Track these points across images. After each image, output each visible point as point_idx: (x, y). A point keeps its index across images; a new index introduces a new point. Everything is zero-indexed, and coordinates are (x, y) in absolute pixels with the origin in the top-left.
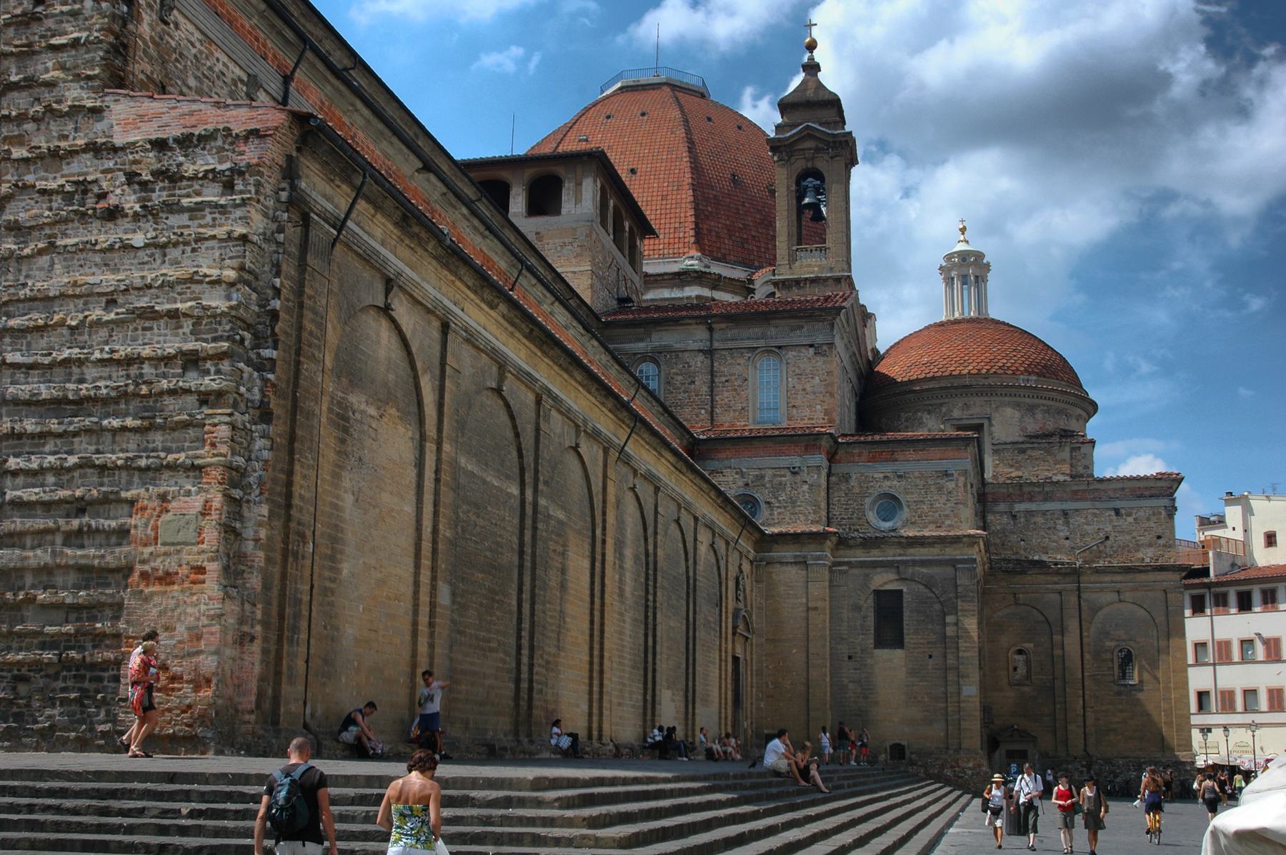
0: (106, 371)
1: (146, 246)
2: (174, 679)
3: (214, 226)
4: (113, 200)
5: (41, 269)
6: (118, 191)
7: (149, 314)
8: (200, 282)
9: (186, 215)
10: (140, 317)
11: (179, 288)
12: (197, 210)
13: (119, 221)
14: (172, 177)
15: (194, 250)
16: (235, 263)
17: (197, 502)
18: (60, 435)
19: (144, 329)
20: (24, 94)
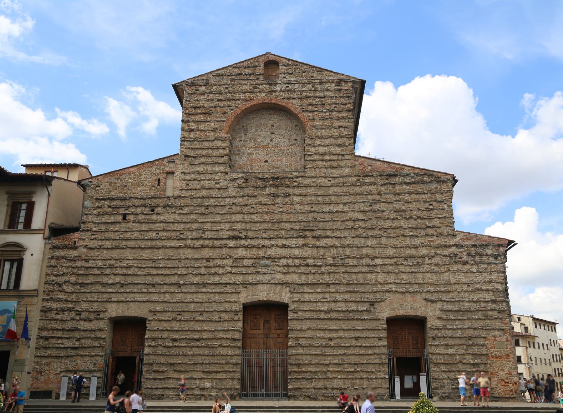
0: (470, 304)
1: (477, 272)
2: (506, 383)
3: (494, 268)
4: (463, 259)
5: (446, 276)
6: (465, 257)
7: (480, 290)
8: (493, 282)
9: (486, 265)
10: (478, 290)
11: (488, 284)
12: (489, 264)
13: (467, 265)
14: (481, 255)
15: (490, 274)
16: (502, 278)
17: (504, 338)
18: (460, 320)
19: (479, 293)
20: (432, 229)
